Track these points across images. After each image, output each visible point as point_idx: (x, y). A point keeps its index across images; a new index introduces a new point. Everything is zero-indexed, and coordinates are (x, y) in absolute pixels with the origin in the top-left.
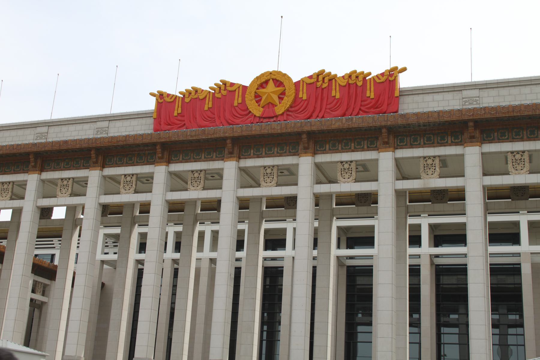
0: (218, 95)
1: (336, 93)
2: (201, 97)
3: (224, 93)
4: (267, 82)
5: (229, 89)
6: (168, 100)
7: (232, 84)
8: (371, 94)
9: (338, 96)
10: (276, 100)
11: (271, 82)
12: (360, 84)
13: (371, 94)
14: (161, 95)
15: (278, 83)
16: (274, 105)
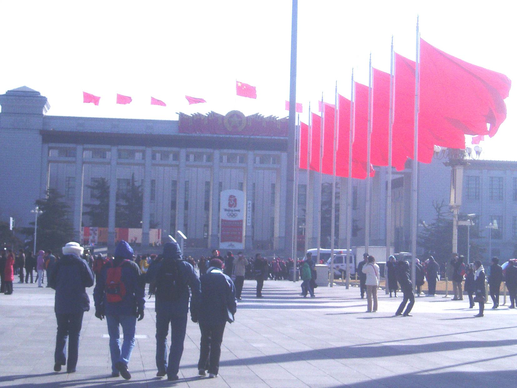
14: (182, 115)
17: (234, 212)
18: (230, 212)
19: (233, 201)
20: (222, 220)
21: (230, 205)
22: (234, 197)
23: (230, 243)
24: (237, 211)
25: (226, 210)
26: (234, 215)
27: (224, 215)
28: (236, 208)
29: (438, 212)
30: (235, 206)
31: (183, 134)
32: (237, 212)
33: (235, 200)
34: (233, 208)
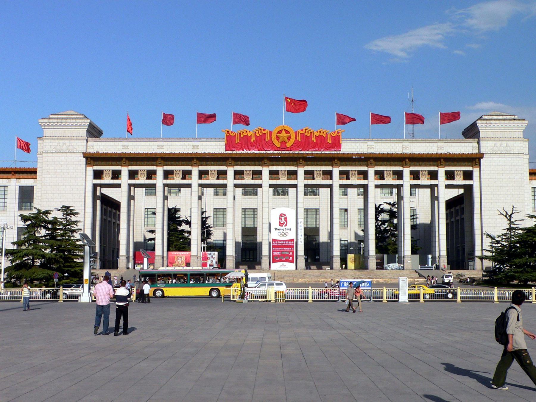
0: (258, 135)
1: (314, 139)
2: (249, 135)
3: (261, 134)
4: (281, 130)
5: (264, 132)
6: (232, 135)
7: (264, 130)
8: (329, 141)
9: (315, 141)
10: (286, 140)
11: (284, 131)
12: (325, 136)
13: (329, 141)
15: (287, 132)
16: (285, 143)
17: (285, 231)
18: (281, 231)
19: (283, 220)
20: (273, 240)
21: (281, 224)
22: (285, 215)
23: (281, 263)
24: (288, 230)
25: (276, 229)
26: (285, 234)
27: (275, 235)
28: (287, 227)
29: (510, 220)
30: (286, 225)
31: (229, 152)
32: (288, 231)
33: (286, 219)
34: (284, 227)
